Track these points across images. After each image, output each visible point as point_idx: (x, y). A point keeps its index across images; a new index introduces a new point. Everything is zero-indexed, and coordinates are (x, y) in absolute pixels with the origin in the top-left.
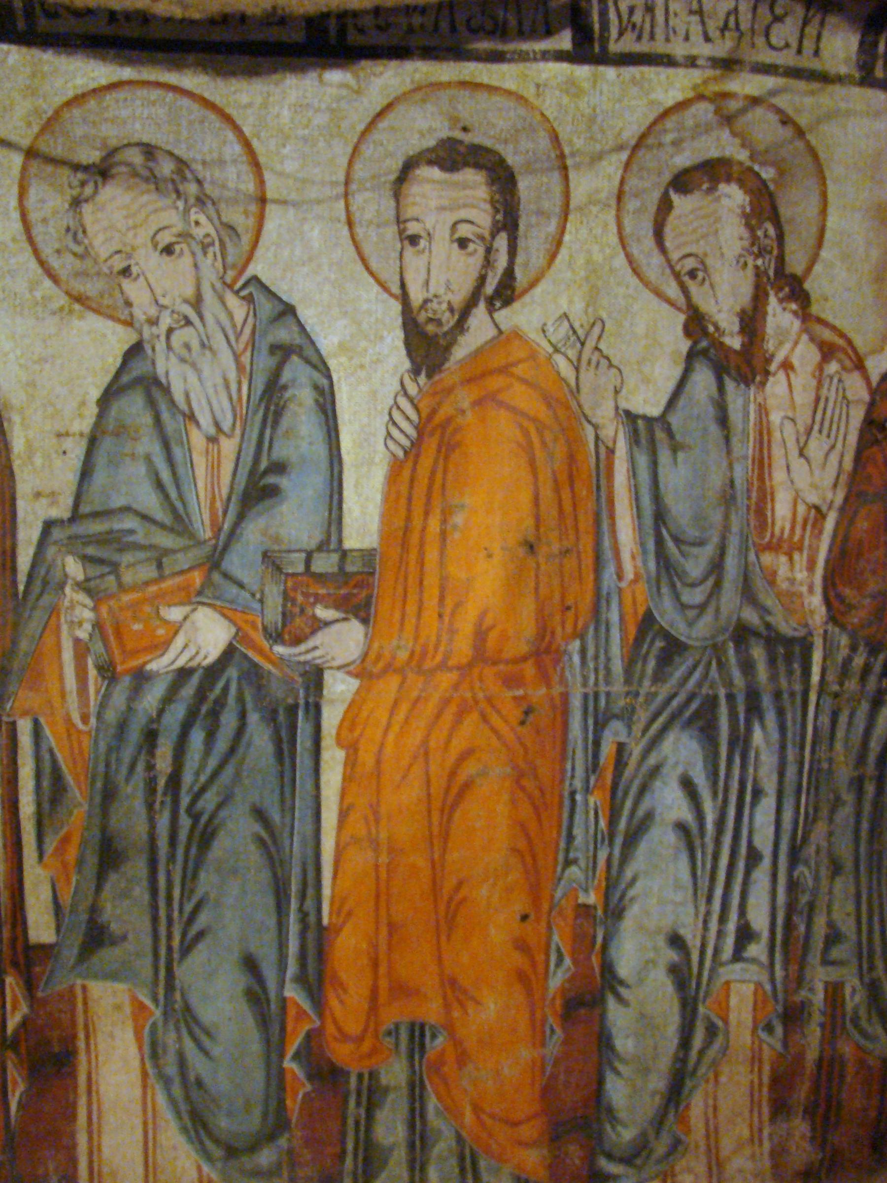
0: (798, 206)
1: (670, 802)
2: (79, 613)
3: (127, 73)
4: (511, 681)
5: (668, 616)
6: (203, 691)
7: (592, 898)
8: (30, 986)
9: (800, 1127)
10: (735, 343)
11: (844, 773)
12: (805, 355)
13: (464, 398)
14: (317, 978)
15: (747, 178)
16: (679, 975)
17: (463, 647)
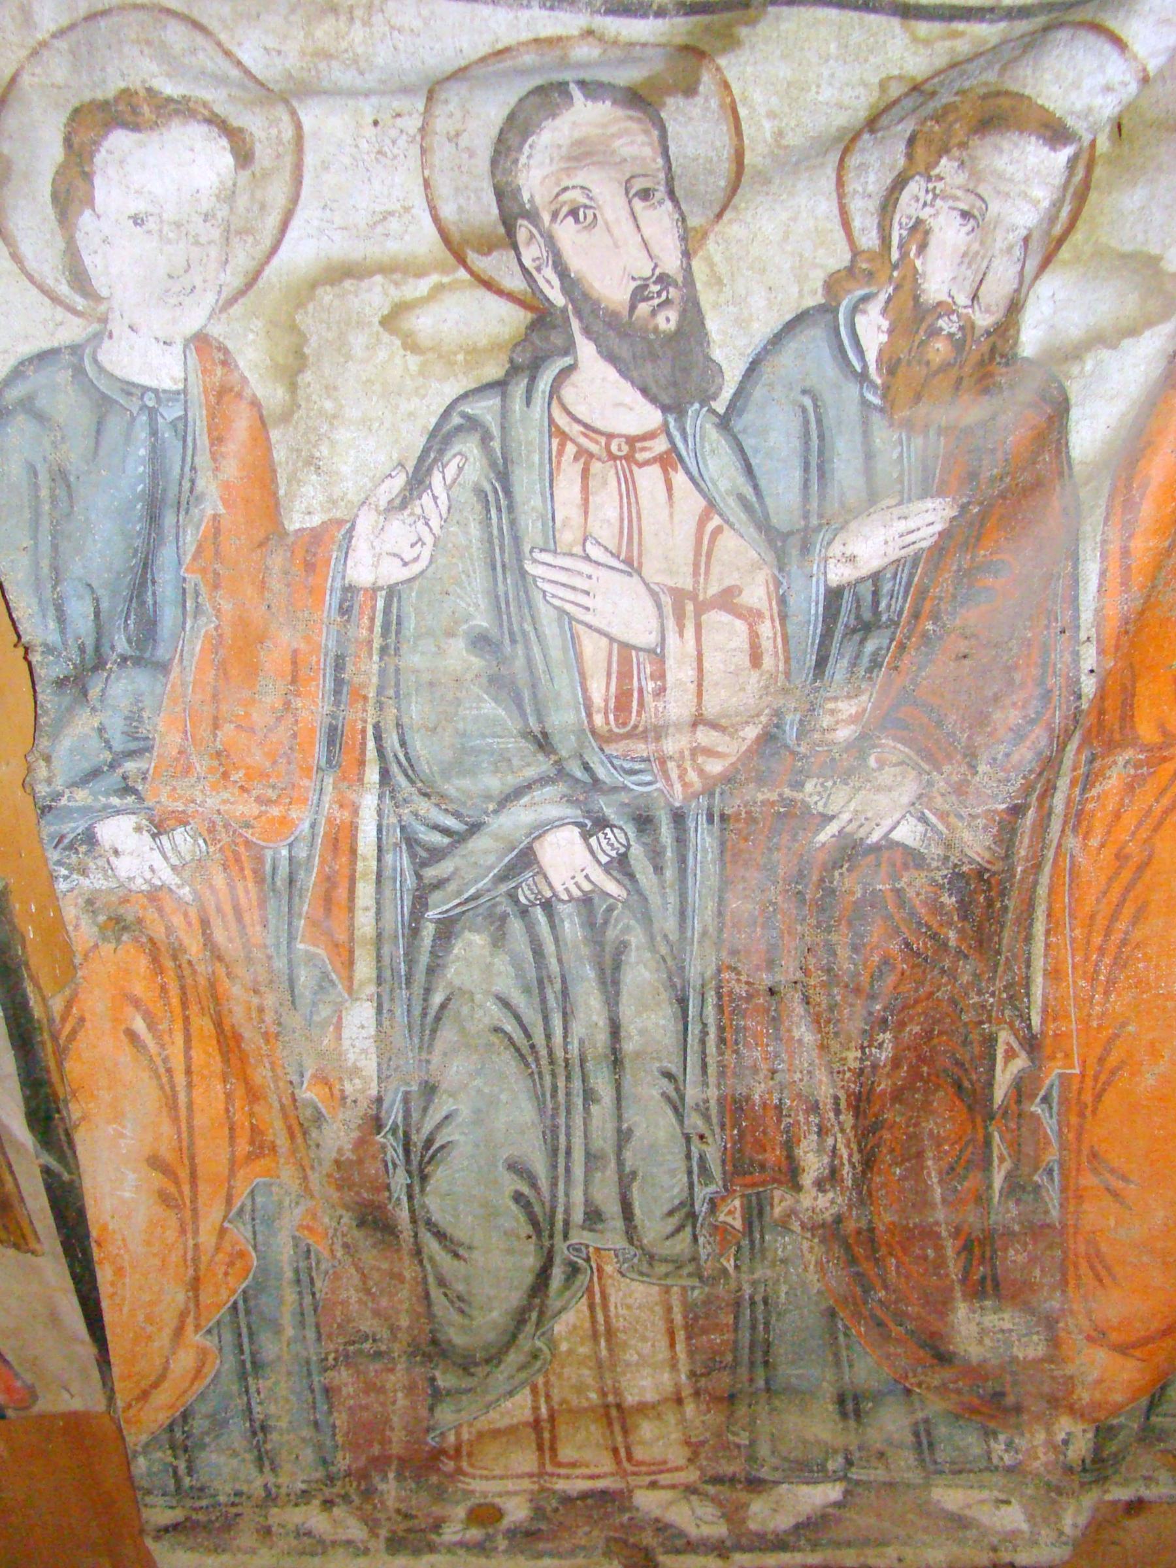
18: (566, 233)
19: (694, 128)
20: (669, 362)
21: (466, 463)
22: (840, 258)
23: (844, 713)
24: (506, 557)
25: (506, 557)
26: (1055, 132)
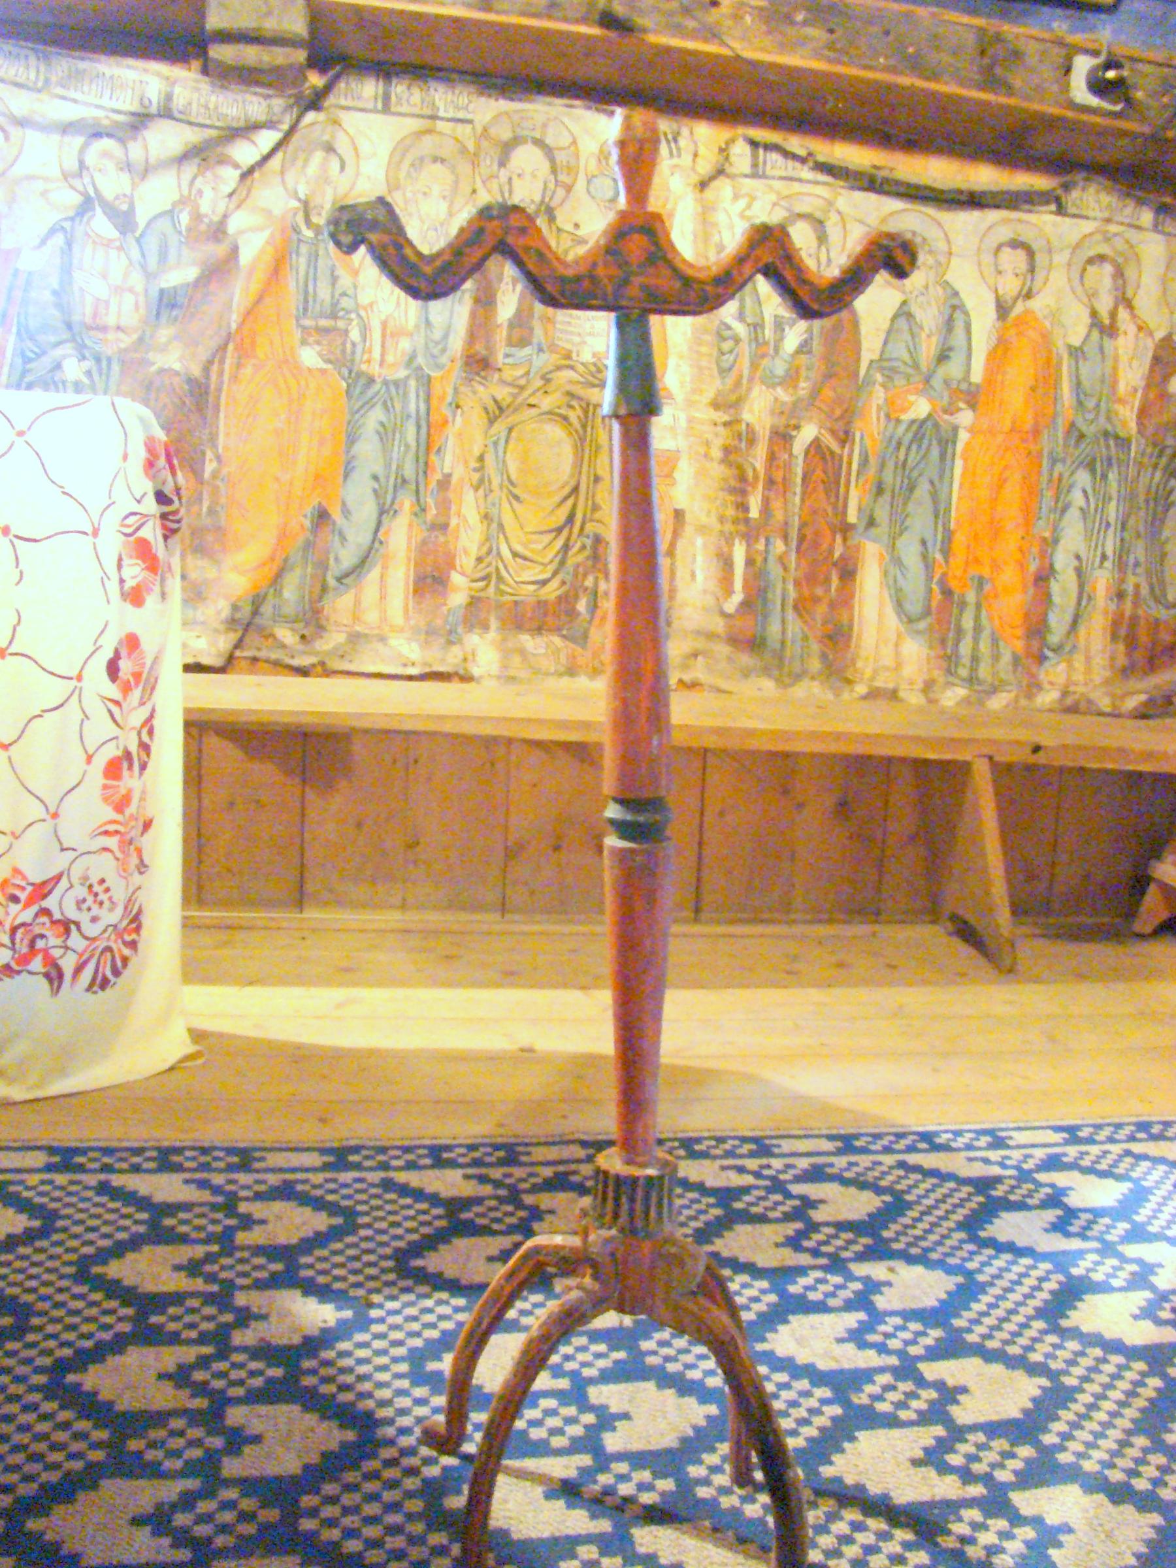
0: (1130, 273)
1: (1077, 498)
2: (879, 395)
3: (908, 206)
4: (1024, 441)
5: (1080, 423)
6: (919, 427)
7: (1047, 534)
8: (845, 539)
9: (1121, 648)
10: (1107, 322)
11: (1142, 498)
12: (1132, 329)
13: (1012, 332)
14: (946, 552)
15: (1114, 262)
16: (1079, 572)
17: (1007, 424)
18: (98, 177)
19: (136, 151)
20: (124, 220)
21: (59, 240)
22: (177, 197)
23: (165, 333)
24: (67, 270)
25: (67, 270)
26: (236, 166)
